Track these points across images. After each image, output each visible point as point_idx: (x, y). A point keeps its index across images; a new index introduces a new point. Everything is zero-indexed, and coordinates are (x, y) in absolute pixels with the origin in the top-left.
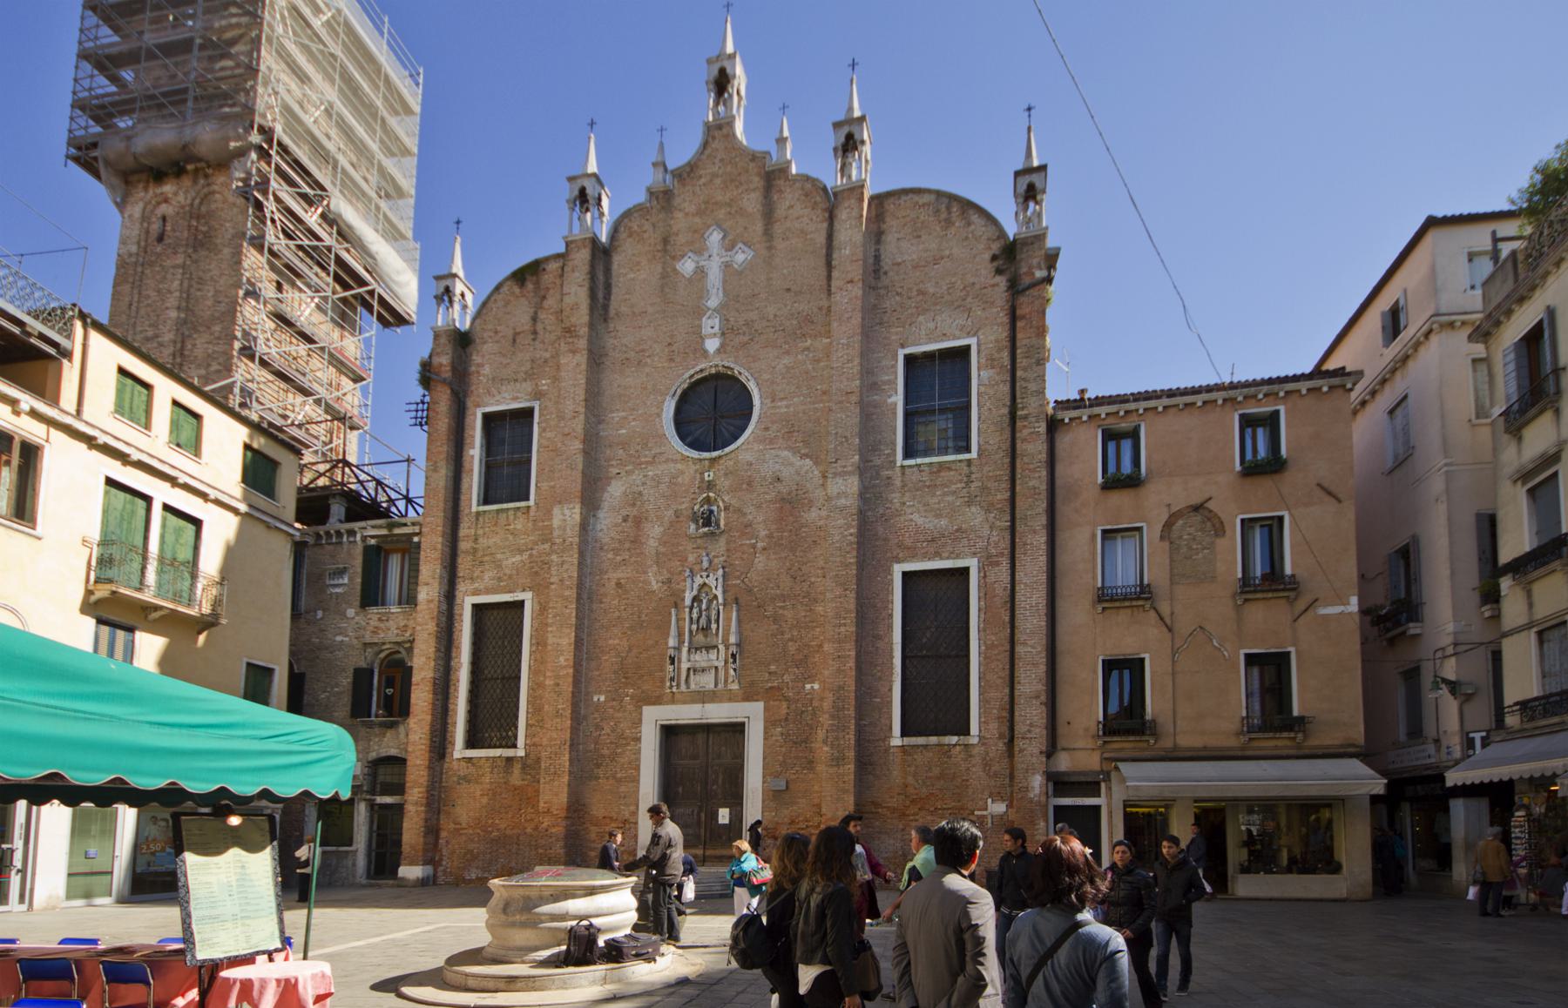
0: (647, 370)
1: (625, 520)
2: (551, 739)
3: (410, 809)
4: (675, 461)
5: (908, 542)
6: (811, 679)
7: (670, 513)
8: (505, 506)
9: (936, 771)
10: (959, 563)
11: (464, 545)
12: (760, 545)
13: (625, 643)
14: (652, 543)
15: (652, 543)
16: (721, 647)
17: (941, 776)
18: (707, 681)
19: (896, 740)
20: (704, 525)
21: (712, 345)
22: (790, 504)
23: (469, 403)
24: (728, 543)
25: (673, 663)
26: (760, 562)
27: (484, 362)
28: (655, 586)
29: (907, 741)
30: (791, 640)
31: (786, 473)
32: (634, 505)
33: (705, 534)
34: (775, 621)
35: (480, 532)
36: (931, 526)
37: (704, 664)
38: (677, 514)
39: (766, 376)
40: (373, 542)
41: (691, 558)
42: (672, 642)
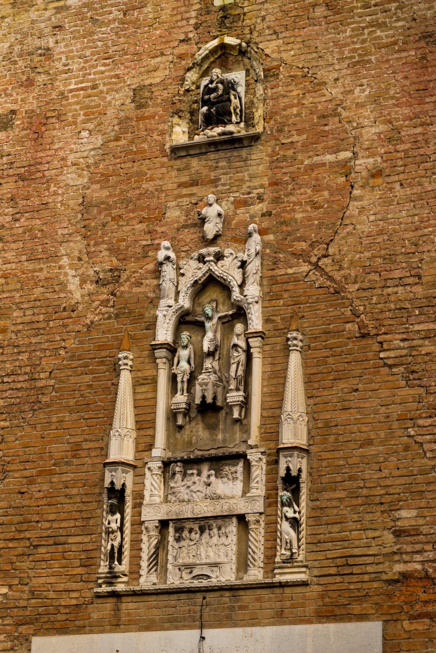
12: (364, 163)
15: (71, 177)
16: (253, 456)
18: (217, 557)
24: (275, 162)
25: (118, 507)
26: (365, 211)
28: (76, 291)
32: (30, 83)
33: (214, 145)
34: (412, 376)
37: (205, 509)
38: (140, 97)
41: (174, 214)
42: (122, 448)
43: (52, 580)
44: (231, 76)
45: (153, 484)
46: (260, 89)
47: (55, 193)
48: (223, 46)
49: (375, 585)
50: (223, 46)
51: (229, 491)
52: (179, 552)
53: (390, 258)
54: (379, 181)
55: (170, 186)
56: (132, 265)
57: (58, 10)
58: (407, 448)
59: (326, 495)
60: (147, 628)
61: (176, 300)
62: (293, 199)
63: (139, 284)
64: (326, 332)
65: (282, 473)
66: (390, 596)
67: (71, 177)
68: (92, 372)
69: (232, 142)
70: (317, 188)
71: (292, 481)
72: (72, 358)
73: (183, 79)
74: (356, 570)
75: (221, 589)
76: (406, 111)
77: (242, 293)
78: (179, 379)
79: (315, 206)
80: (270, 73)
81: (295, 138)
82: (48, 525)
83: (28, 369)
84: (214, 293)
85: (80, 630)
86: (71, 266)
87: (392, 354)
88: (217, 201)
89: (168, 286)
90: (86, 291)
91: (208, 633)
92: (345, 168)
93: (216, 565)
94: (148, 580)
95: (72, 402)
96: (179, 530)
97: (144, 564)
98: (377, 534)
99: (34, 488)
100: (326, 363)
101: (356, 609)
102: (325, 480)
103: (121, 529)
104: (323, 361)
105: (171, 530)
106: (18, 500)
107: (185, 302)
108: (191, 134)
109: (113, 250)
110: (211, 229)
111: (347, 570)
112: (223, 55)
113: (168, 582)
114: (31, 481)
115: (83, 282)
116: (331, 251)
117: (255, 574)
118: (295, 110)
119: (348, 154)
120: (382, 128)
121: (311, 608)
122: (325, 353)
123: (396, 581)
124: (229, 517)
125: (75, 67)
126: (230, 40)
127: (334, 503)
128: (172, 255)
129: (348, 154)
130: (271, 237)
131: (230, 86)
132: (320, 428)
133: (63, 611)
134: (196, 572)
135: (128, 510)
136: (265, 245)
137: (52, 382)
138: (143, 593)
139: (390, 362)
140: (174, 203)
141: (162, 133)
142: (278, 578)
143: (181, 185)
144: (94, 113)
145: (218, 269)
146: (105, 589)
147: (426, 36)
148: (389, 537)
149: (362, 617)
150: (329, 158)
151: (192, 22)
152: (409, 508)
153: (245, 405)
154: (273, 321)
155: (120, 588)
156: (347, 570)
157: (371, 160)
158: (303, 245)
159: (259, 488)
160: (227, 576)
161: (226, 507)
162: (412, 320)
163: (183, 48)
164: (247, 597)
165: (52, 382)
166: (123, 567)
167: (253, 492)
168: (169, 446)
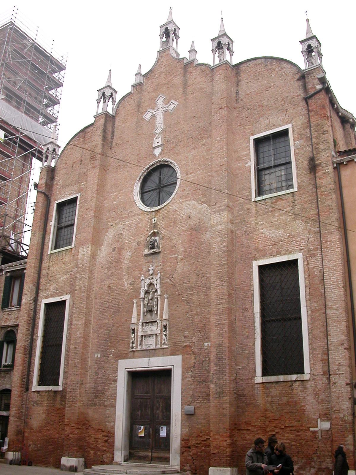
0: (128, 169)
1: (114, 250)
2: (72, 381)
3: (12, 419)
4: (139, 215)
5: (261, 247)
6: (207, 338)
7: (135, 244)
8: (61, 249)
9: (285, 399)
10: (291, 257)
11: (44, 272)
12: (180, 257)
14: (126, 262)
15: (126, 262)
16: (158, 321)
17: (288, 403)
18: (151, 343)
19: (259, 379)
20: (151, 248)
21: (157, 152)
22: (196, 230)
23: (52, 200)
25: (133, 333)
26: (180, 267)
27: (59, 179)
28: (127, 286)
31: (193, 215)
32: (118, 241)
35: (51, 264)
36: (273, 235)
37: (149, 333)
38: (139, 244)
40: (8, 274)
41: (144, 269)
42: (134, 320)
44: (156, 238)
45: (140, 327)
46: (161, 241)
50: (154, 232)
51: (155, 329)
53: (184, 278)
56: (137, 281)
57: (124, 225)
59: (172, 329)
63: (138, 285)
64: (173, 294)
65: (163, 325)
66: (183, 350)
69: (155, 253)
70: (171, 263)
71: (165, 327)
72: (126, 301)
73: (147, 239)
75: (152, 349)
76: (188, 245)
79: (171, 267)
80: (163, 238)
84: (152, 286)
85: (127, 358)
86: (126, 281)
88: (152, 266)
89: (143, 285)
91: (151, 358)
92: (176, 258)
94: (139, 348)
96: (145, 337)
97: (139, 345)
101: (177, 353)
102: (171, 326)
103: (134, 337)
104: (172, 300)
105: (143, 337)
106: (116, 332)
109: (134, 277)
110: (151, 272)
112: (154, 234)
114: (118, 327)
115: (128, 284)
117: (158, 346)
119: (177, 255)
121: (169, 353)
122: (172, 299)
126: (156, 231)
128: (144, 278)
129: (177, 255)
131: (156, 240)
132: (171, 315)
135: (135, 333)
136: (161, 275)
138: (138, 351)
143: (146, 263)
144: (130, 247)
145: (152, 281)
146: (132, 350)
147: (192, 229)
148: (183, 338)
149: (178, 355)
150: (174, 256)
153: (157, 310)
155: (134, 350)
158: (168, 275)
159: (159, 328)
160: (153, 347)
164: (157, 351)
166: (134, 345)
167: (158, 329)
168: (143, 320)
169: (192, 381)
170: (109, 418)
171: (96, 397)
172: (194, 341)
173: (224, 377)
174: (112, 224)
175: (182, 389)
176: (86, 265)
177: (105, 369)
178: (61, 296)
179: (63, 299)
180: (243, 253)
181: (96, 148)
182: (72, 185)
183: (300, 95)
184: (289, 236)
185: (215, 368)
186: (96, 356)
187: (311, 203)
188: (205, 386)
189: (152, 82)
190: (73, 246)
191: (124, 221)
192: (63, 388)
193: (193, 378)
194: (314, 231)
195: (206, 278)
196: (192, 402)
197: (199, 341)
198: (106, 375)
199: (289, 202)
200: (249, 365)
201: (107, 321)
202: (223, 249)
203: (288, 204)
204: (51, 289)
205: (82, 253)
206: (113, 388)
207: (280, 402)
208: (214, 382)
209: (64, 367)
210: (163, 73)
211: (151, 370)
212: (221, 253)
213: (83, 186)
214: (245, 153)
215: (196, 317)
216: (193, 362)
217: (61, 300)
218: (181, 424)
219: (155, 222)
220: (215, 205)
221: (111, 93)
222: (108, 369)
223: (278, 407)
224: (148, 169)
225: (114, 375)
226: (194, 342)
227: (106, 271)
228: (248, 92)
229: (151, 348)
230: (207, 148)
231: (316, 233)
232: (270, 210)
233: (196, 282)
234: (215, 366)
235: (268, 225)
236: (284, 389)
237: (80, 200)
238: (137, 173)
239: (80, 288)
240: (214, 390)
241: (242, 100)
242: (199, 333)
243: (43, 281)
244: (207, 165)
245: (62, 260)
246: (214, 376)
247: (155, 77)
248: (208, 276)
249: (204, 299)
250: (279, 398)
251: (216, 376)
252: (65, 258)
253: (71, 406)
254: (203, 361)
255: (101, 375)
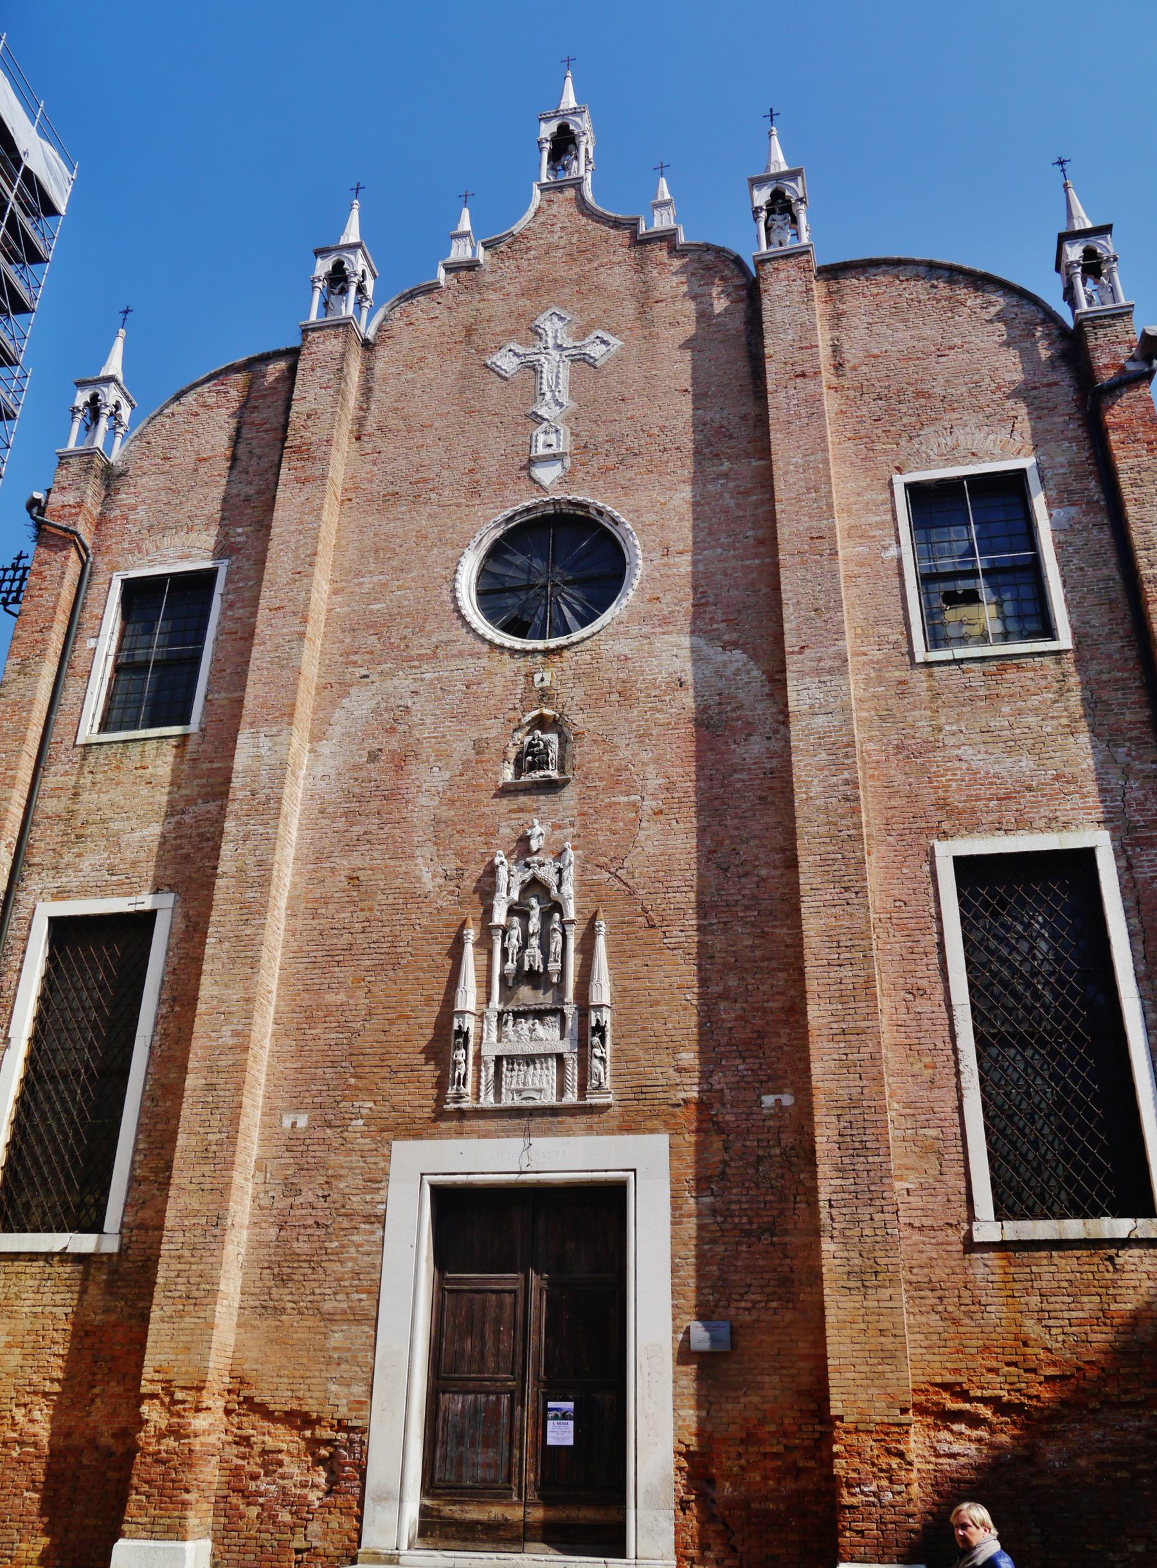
1: (373, 757)
4: (478, 656)
5: (957, 800)
11: (48, 805)
12: (649, 804)
13: (361, 1000)
18: (540, 1085)
28: (429, 882)
29: (1016, 1230)
30: (724, 996)
32: (393, 730)
38: (479, 747)
39: (648, 518)
41: (505, 831)
43: (409, 1098)
47: (412, 811)
48: (541, 716)
49: (663, 1107)
50: (541, 716)
52: (512, 1079)
54: (662, 817)
55: (502, 811)
58: (685, 1009)
60: (485, 1137)
61: (508, 894)
62: (596, 826)
67: (424, 800)
68: (441, 943)
70: (614, 820)
72: (425, 932)
74: (648, 1096)
76: (680, 770)
77: (559, 891)
78: (510, 952)
81: (598, 783)
82: (406, 1056)
83: (390, 939)
85: (431, 1137)
86: (425, 865)
87: (673, 940)
90: (436, 884)
91: (533, 1140)
93: (540, 1091)
94: (488, 1101)
95: (425, 965)
98: (664, 1070)
99: (394, 1028)
100: (623, 945)
101: (649, 1124)
103: (465, 1061)
106: (382, 1037)
107: (515, 895)
108: (517, 775)
111: (644, 1096)
113: (504, 1101)
114: (391, 1022)
115: (434, 877)
116: (625, 865)
117: (571, 1098)
118: (597, 764)
120: (662, 781)
122: (624, 937)
123: (679, 1105)
124: (550, 1055)
125: (428, 721)
126: (548, 712)
127: (631, 1047)
130: (580, 852)
132: (621, 991)
133: (417, 1121)
134: (525, 1095)
137: (409, 949)
139: (671, 946)
140: (505, 824)
141: (496, 773)
142: (589, 1101)
143: (511, 811)
146: (452, 1106)
149: (653, 1131)
151: (519, 696)
152: (687, 1051)
153: (562, 973)
154: (582, 913)
155: (463, 1105)
156: (644, 1096)
157: (654, 803)
161: (548, 1047)
162: (687, 917)
163: (512, 714)
165: (409, 949)
169: (715, 1227)
170: (344, 1366)
171: (283, 1280)
172: (717, 1087)
173: (877, 1217)
174: (366, 673)
175: (674, 1256)
176: (267, 791)
177: (330, 1172)
178: (130, 894)
179: (140, 907)
180: (893, 811)
181: (309, 423)
182: (190, 529)
183: (1056, 384)
184: (1057, 778)
185: (839, 1182)
186: (287, 1123)
187: (1122, 689)
188: (771, 1249)
189: (518, 267)
190: (193, 727)
191: (415, 667)
192: (121, 1245)
193: (719, 1219)
194: (1141, 771)
195: (755, 879)
196: (716, 1306)
197: (737, 1087)
198: (335, 1196)
199: (1045, 677)
200: (945, 1177)
201: (342, 997)
202: (841, 788)
203: (1043, 683)
204: (85, 865)
205: (252, 751)
206: (366, 1248)
207: (1074, 1314)
208: (836, 1233)
209: (133, 1162)
210: (557, 248)
211: (538, 1182)
212: (834, 800)
213: (239, 539)
214: (878, 519)
215: (722, 1005)
216: (716, 1159)
217: (131, 909)
218: (674, 1388)
219: (546, 683)
220: (800, 653)
221: (363, 271)
222: (343, 1172)
223: (1068, 1329)
224: (510, 519)
225: (368, 1198)
226: (722, 1090)
227: (340, 824)
228: (876, 351)
229: (538, 1103)
230: (738, 486)
231: (1148, 777)
232: (981, 693)
233: (718, 890)
234: (835, 1174)
235: (978, 738)
236: (1086, 1268)
237: (228, 581)
238: (467, 527)
239: (241, 870)
240: (838, 1262)
241: (854, 368)
242: (738, 1061)
243: (44, 838)
244: (741, 537)
245: (141, 771)
246: (834, 1212)
247: (529, 256)
248: (763, 872)
249: (752, 947)
250: (1069, 1299)
251: (844, 1211)
252: (155, 767)
253: (181, 1314)
254: (760, 1159)
255: (308, 1196)
